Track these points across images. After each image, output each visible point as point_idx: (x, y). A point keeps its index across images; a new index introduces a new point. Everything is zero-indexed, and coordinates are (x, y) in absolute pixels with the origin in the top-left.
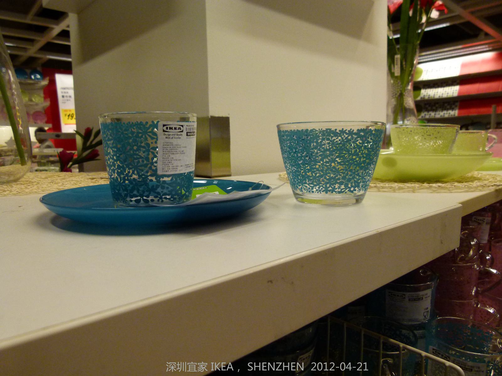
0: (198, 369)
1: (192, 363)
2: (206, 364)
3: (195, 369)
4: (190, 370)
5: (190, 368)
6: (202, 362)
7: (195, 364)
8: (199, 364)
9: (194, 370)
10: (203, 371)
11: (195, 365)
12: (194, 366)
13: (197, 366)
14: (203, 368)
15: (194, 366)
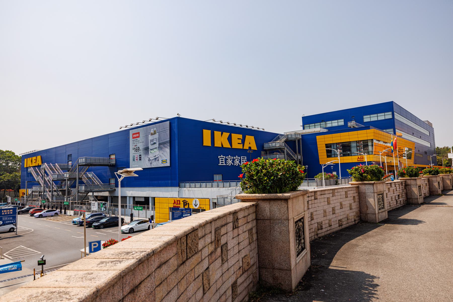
0: (227, 163)
3: (224, 162)
4: (221, 163)
6: (229, 156)
7: (224, 158)
9: (223, 163)
10: (230, 165)
11: (224, 159)
12: (223, 159)
13: (226, 160)
14: (230, 162)
15: (223, 159)
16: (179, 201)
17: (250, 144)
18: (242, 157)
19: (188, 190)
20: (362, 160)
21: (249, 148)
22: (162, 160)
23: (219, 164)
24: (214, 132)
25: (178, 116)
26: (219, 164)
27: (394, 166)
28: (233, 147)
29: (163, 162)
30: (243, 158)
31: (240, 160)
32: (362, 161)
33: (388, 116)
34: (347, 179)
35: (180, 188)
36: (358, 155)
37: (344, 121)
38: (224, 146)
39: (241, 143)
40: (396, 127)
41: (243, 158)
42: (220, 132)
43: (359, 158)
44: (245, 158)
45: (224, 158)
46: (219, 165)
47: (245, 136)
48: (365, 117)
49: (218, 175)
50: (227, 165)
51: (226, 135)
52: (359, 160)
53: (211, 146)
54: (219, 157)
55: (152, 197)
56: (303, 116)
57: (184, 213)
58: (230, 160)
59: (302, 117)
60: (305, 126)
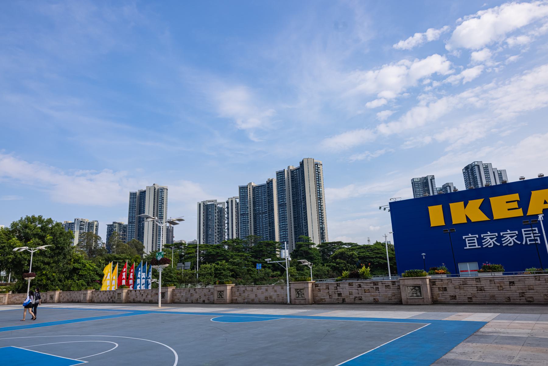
0: (483, 244)
1: (470, 235)
3: (476, 244)
4: (469, 246)
6: (488, 232)
7: (476, 237)
9: (475, 246)
10: (492, 246)
11: (475, 238)
12: (474, 240)
13: (480, 240)
15: (474, 240)
18: (523, 230)
25: (392, 201)
28: (495, 218)
30: (525, 231)
38: (473, 220)
41: (525, 231)
42: (463, 203)
44: (535, 230)
46: (465, 248)
49: (468, 264)
50: (484, 246)
54: (464, 237)
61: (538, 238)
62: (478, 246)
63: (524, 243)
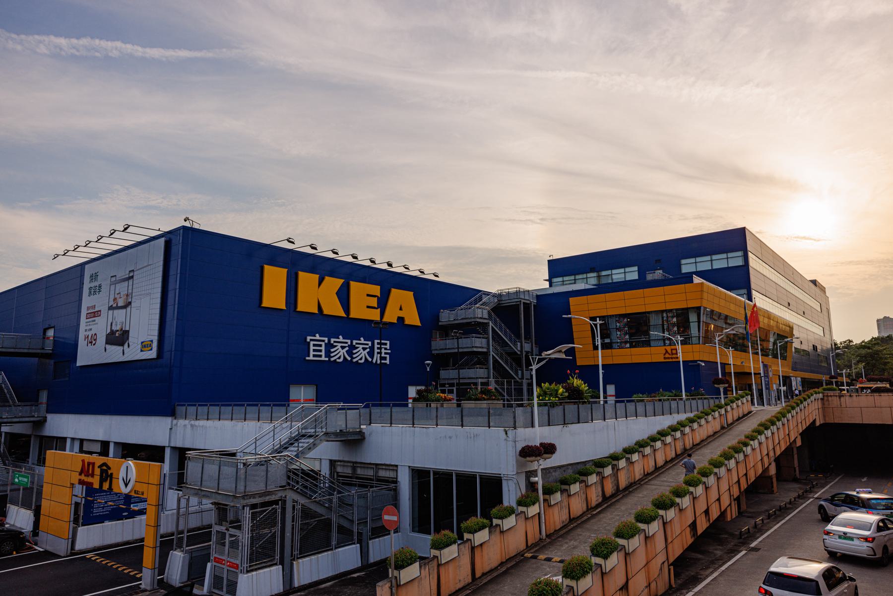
0: (332, 355)
1: (318, 337)
2: (347, 343)
3: (323, 353)
4: (314, 356)
5: (314, 350)
7: (323, 341)
8: (335, 342)
9: (321, 356)
10: (341, 360)
11: (323, 344)
12: (321, 346)
13: (329, 346)
14: (341, 354)
15: (321, 346)
16: (93, 464)
17: (401, 309)
19: (192, 426)
20: (675, 358)
21: (398, 320)
22: (142, 343)
23: (309, 356)
24: (297, 275)
25: (187, 224)
26: (309, 356)
27: (751, 373)
28: (352, 315)
29: (145, 346)
31: (372, 348)
32: (674, 360)
33: (735, 260)
34: (623, 404)
35: (175, 419)
36: (665, 345)
37: (639, 271)
38: (325, 312)
39: (376, 306)
40: (753, 286)
43: (667, 351)
44: (386, 344)
45: (323, 341)
46: (307, 358)
47: (389, 291)
48: (683, 261)
50: (332, 359)
51: (334, 284)
52: (668, 358)
53: (285, 308)
54: (309, 338)
55: (116, 443)
56: (551, 258)
57: (132, 500)
58: (364, 349)
59: (548, 261)
60: (555, 280)
61: (388, 356)
62: (325, 357)
63: (374, 361)
